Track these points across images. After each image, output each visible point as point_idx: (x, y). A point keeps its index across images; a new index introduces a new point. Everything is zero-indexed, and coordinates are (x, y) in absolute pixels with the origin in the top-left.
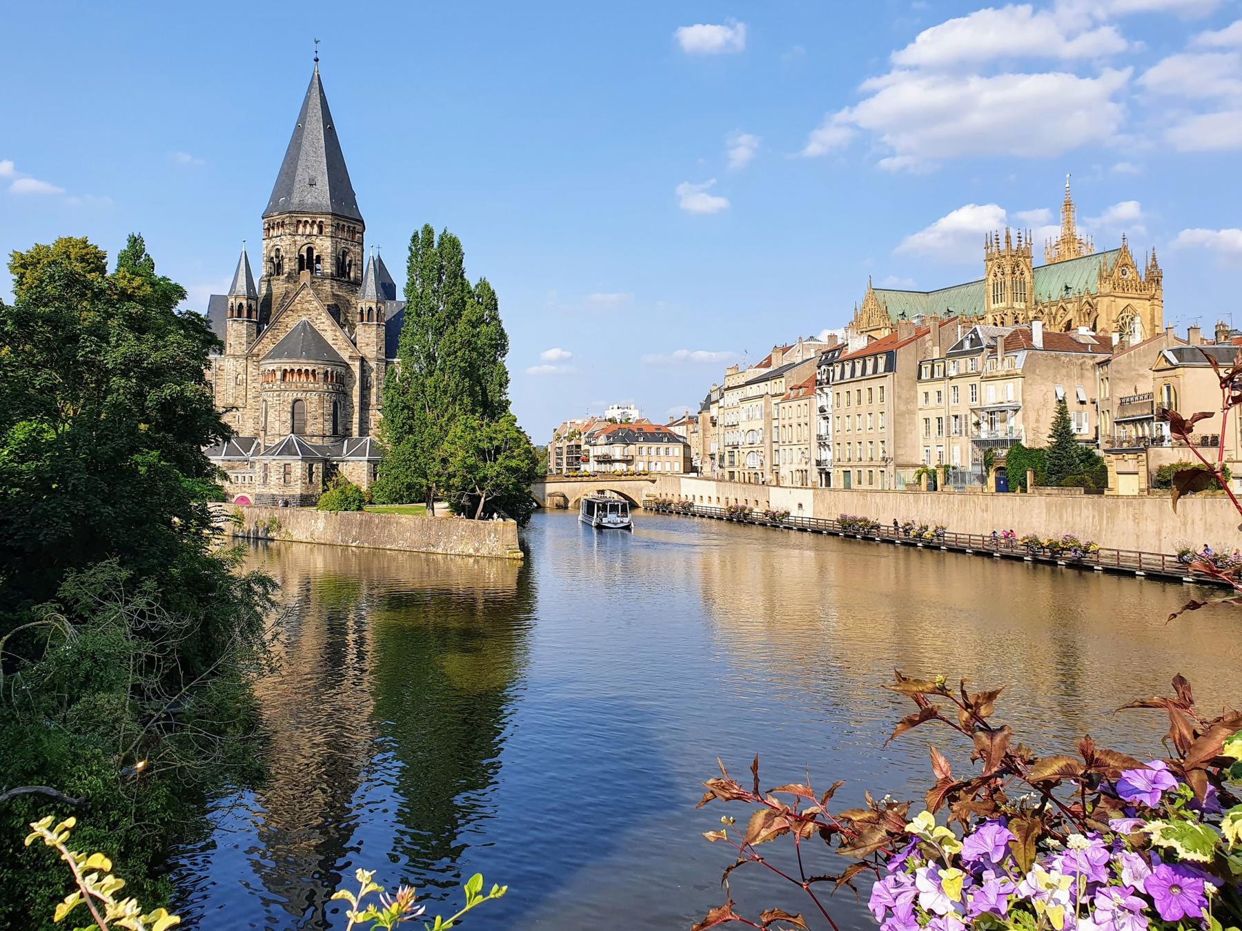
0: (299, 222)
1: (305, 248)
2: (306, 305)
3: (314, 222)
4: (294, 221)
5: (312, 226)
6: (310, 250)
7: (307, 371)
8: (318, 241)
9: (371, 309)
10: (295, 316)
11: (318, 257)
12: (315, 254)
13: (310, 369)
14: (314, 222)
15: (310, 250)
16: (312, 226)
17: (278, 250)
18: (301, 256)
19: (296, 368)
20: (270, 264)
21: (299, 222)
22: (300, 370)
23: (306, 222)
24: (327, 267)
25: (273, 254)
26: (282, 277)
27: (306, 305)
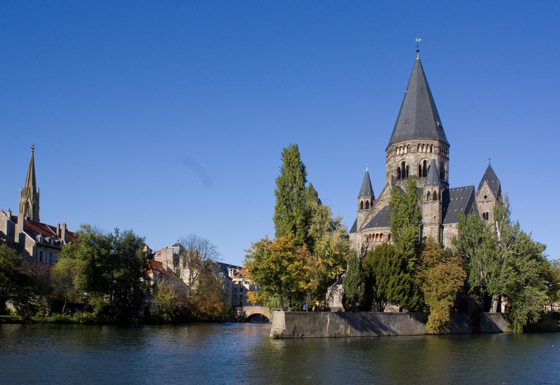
0: (397, 148)
1: (401, 162)
3: (405, 146)
4: (395, 148)
6: (403, 163)
7: (377, 235)
8: (407, 157)
9: (429, 192)
10: (383, 203)
11: (408, 166)
12: (406, 165)
14: (405, 146)
15: (403, 163)
18: (399, 168)
21: (397, 148)
22: (374, 235)
23: (401, 147)
24: (413, 172)
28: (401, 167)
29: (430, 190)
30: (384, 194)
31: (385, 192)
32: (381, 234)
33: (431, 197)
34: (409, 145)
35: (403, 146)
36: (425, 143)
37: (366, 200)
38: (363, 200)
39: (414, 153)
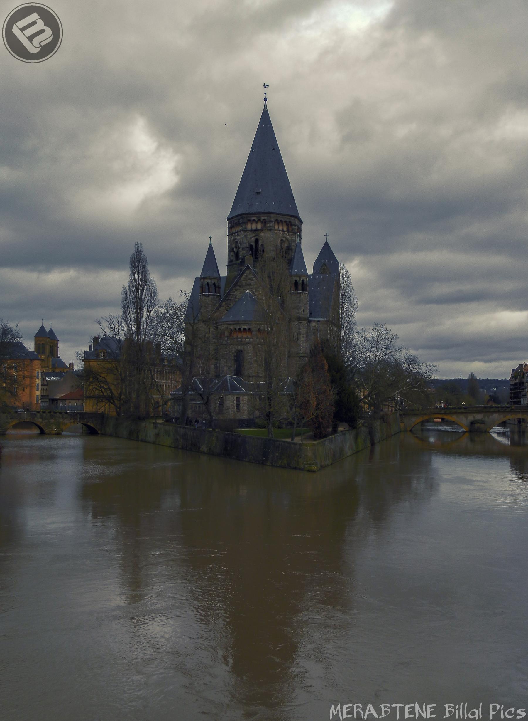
1: (253, 239)
2: (249, 281)
5: (257, 223)
6: (257, 241)
8: (262, 234)
13: (246, 327)
15: (257, 241)
16: (257, 223)
17: (237, 242)
19: (238, 327)
20: (232, 253)
21: (249, 220)
23: (254, 220)
25: (234, 246)
26: (238, 262)
27: (249, 281)
28: (254, 244)
29: (298, 279)
30: (242, 278)
31: (243, 277)
32: (249, 329)
33: (300, 287)
34: (264, 219)
35: (256, 219)
36: (282, 219)
37: (213, 282)
38: (209, 281)
39: (271, 230)
